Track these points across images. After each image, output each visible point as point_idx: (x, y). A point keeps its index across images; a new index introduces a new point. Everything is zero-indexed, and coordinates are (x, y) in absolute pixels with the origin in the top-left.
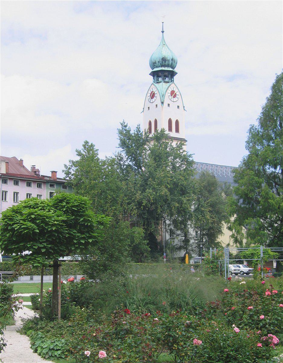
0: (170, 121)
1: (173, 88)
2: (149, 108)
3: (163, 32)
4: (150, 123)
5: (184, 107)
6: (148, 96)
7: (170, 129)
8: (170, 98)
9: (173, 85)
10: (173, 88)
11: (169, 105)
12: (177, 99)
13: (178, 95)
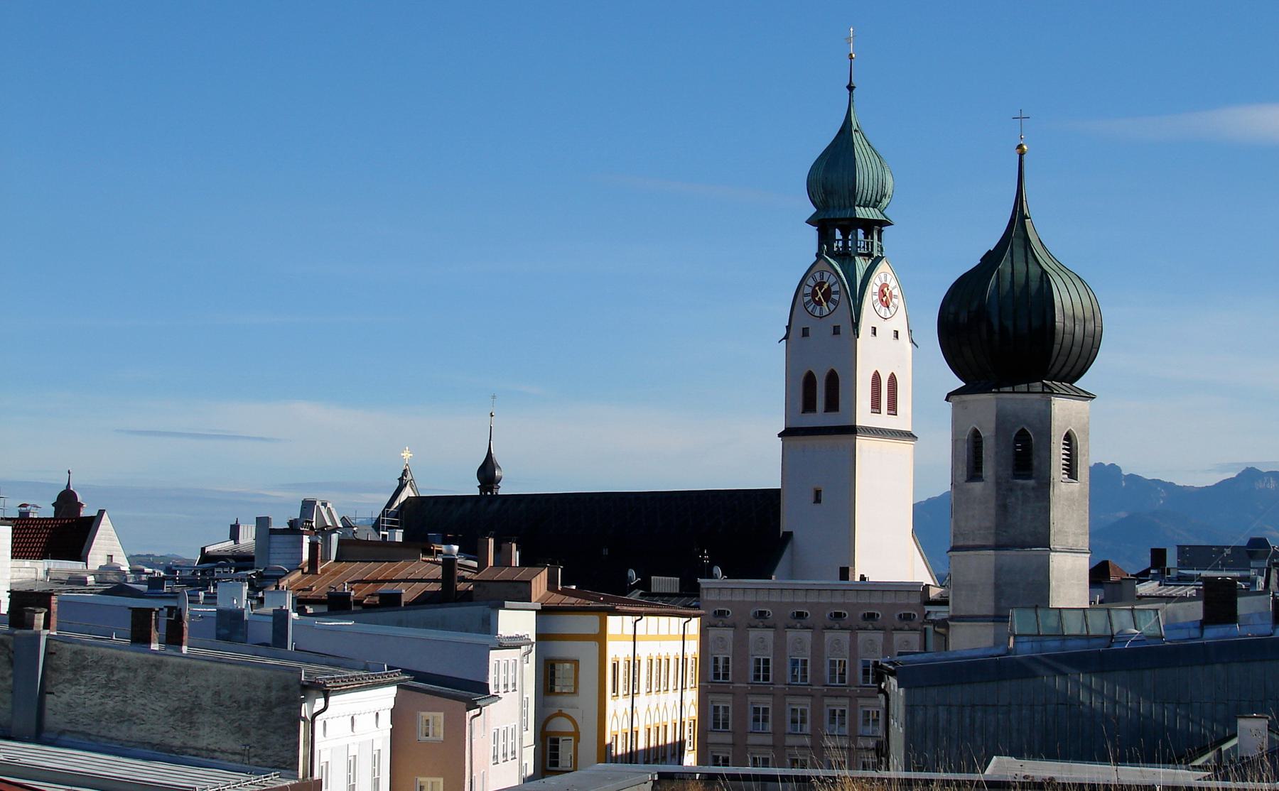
0: (876, 378)
1: (886, 277)
2: (805, 332)
3: (851, 88)
4: (810, 380)
5: (911, 331)
6: (806, 295)
7: (876, 406)
10: (886, 277)
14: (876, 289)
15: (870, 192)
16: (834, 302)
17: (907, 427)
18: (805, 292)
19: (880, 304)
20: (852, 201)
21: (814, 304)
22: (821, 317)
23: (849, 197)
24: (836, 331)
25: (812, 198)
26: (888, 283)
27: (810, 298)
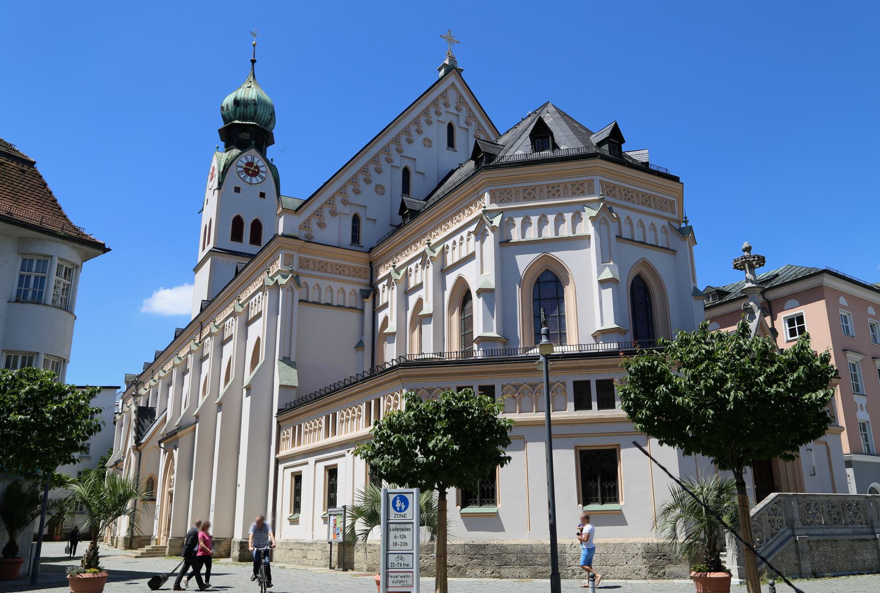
16: (261, 177)
21: (245, 174)
22: (251, 184)
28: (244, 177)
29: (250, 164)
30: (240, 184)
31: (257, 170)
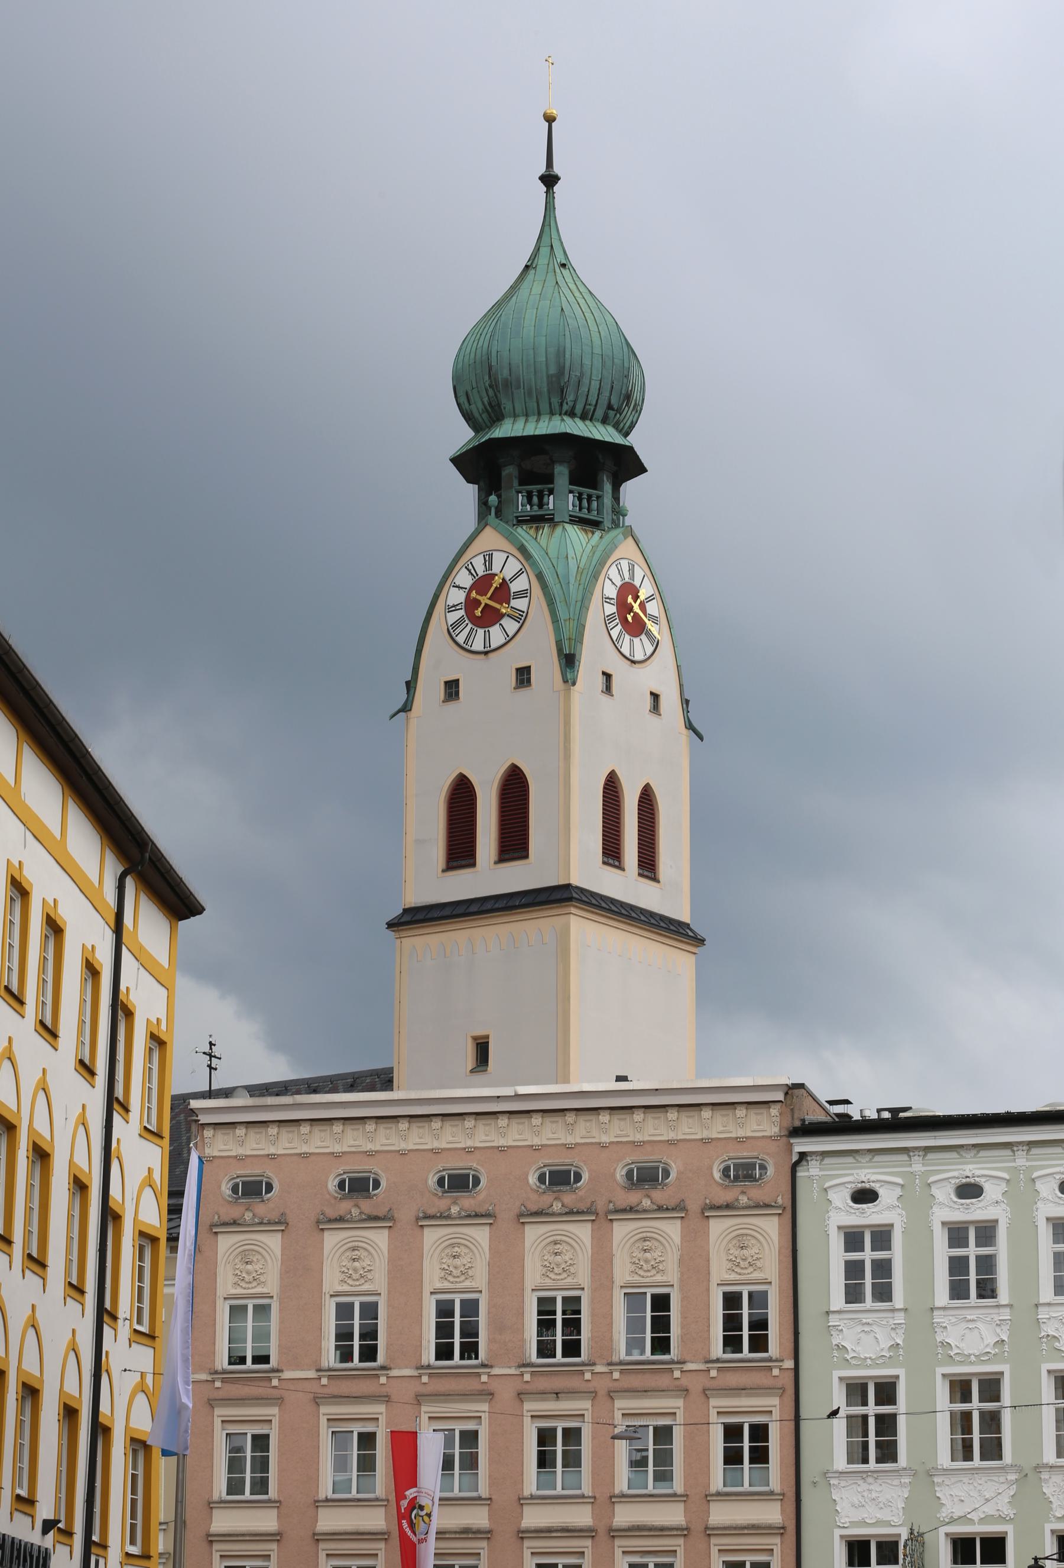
0: (612, 788)
1: (631, 570)
2: (452, 689)
5: (687, 702)
8: (615, 633)
9: (627, 549)
10: (631, 570)
11: (608, 676)
12: (650, 649)
13: (654, 619)
14: (612, 592)
15: (595, 385)
17: (683, 915)
18: (450, 603)
19: (619, 627)
20: (555, 401)
21: (470, 626)
22: (486, 653)
23: (549, 392)
24: (523, 676)
25: (466, 406)
26: (637, 583)
27: (462, 612)
28: (466, 641)
29: (482, 584)
30: (458, 666)
31: (474, 594)
